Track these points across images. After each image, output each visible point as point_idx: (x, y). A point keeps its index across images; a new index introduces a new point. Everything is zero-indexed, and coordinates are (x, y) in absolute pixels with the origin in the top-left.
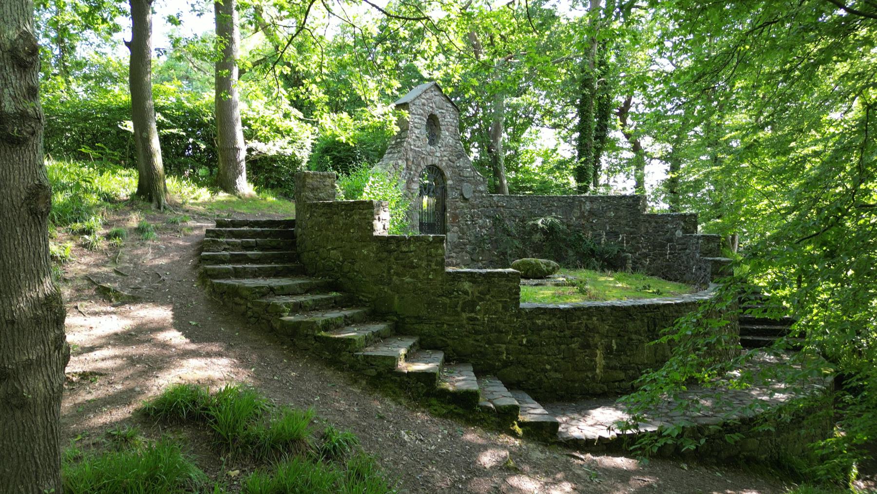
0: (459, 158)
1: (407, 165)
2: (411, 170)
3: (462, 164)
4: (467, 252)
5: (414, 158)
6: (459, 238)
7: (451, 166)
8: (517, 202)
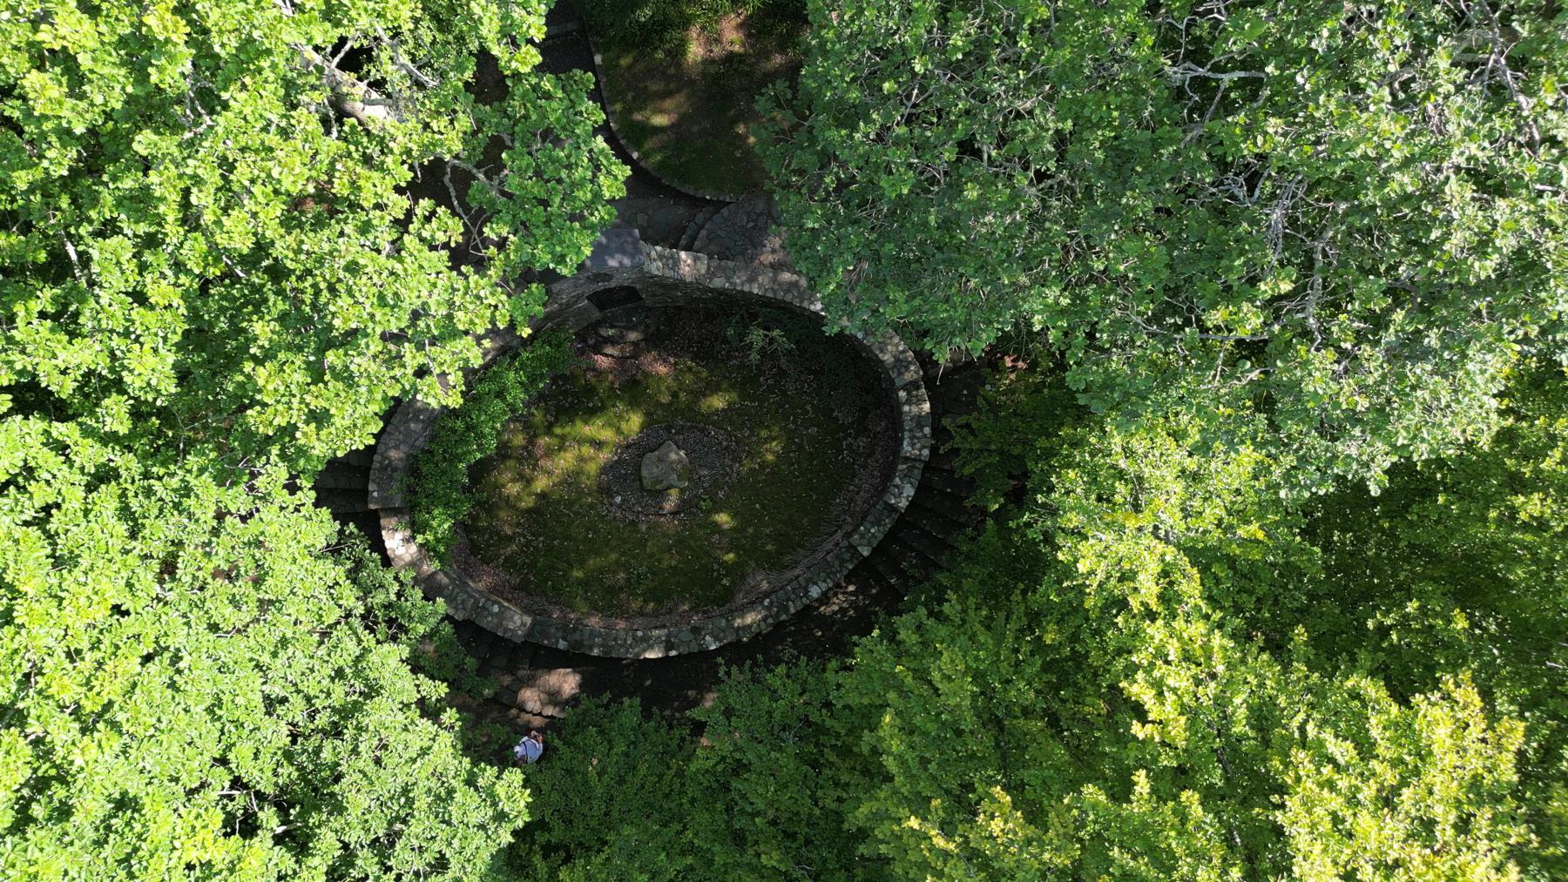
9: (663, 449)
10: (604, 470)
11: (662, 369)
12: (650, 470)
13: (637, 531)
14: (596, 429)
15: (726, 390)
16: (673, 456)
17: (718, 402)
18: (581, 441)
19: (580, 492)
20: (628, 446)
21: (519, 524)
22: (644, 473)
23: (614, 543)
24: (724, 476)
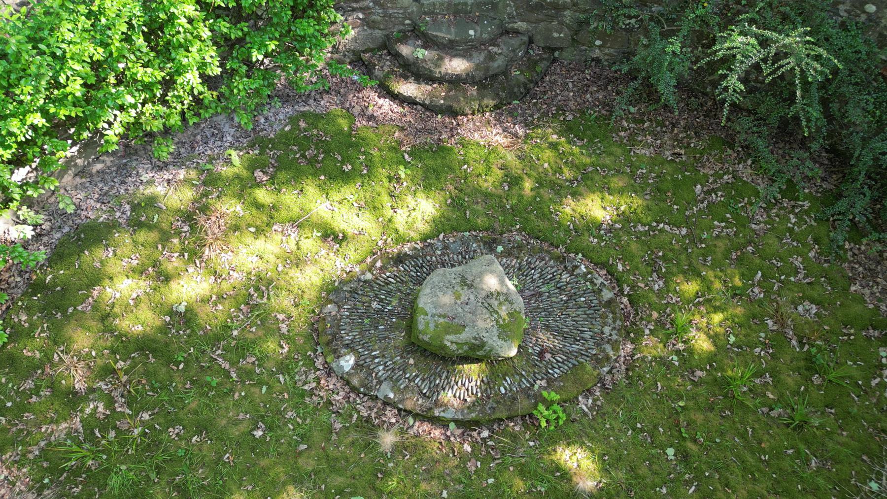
4: (561, 23)
9: (473, 268)
10: (333, 291)
11: (496, 137)
12: (436, 299)
13: (370, 446)
14: (336, 206)
15: (621, 192)
16: (491, 282)
17: (597, 208)
18: (299, 223)
19: (266, 321)
20: (400, 259)
21: (108, 372)
22: (425, 301)
23: (308, 464)
24: (598, 362)
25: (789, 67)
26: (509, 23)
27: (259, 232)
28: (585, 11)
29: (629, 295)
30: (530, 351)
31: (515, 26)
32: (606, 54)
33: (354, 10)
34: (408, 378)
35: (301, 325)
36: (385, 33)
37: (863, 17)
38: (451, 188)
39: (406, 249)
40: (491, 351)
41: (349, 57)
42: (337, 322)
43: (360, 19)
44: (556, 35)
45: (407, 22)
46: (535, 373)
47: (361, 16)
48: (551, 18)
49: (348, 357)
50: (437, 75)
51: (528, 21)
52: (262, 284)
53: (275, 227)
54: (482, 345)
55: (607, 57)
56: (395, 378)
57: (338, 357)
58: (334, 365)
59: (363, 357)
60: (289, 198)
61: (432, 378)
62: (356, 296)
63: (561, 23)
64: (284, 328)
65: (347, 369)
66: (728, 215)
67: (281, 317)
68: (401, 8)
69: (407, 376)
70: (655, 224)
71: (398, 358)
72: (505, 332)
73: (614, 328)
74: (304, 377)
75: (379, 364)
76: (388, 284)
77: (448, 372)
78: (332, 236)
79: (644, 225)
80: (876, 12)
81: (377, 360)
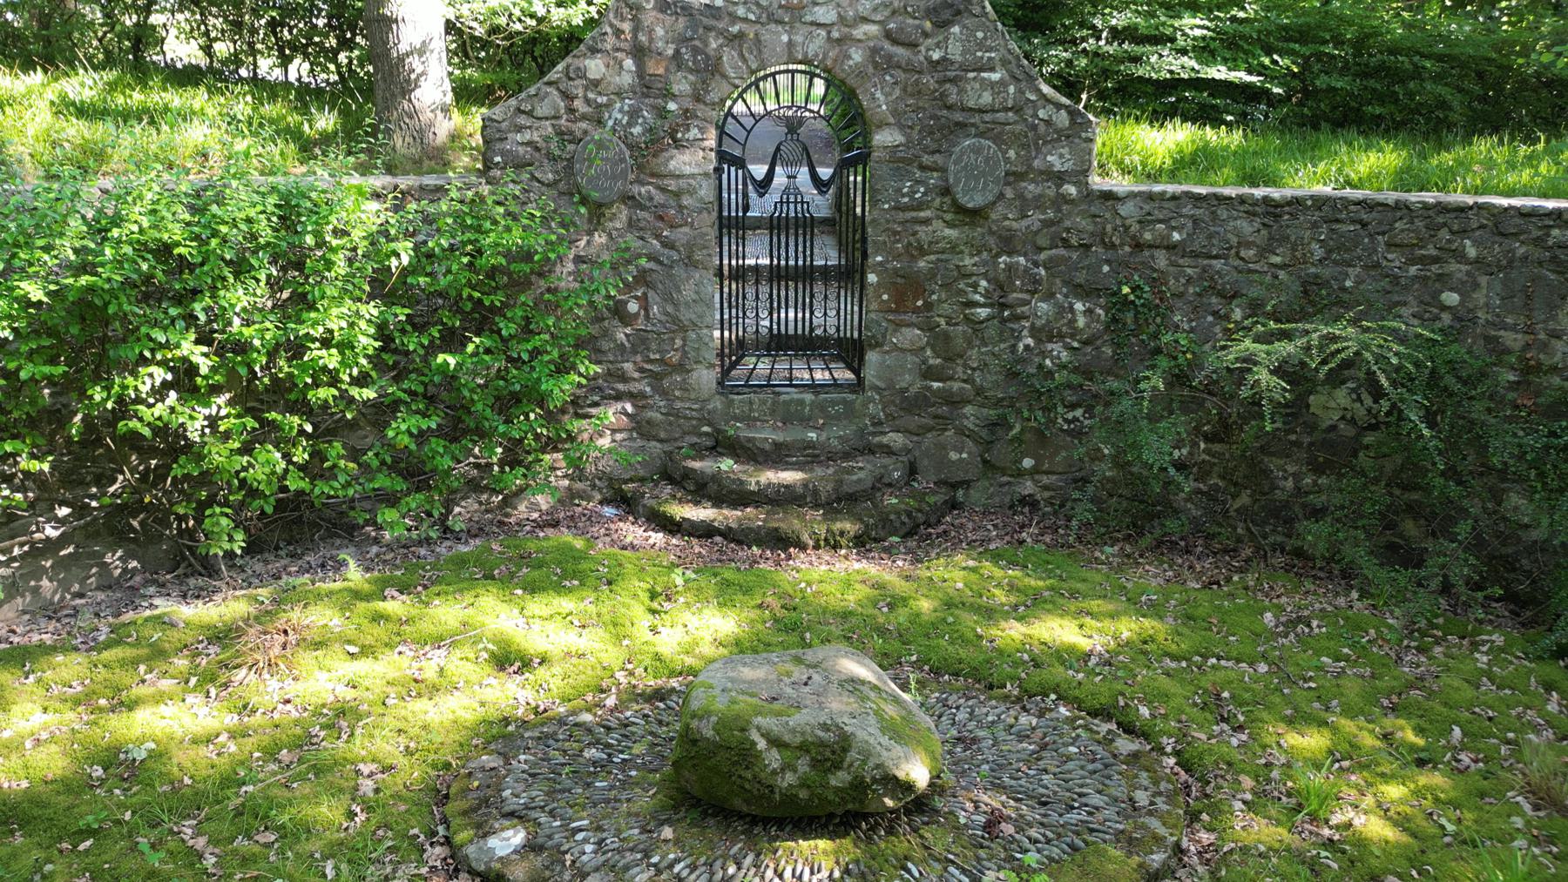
0: (942, 25)
1: (641, 72)
2: (669, 95)
3: (955, 51)
4: (961, 432)
5: (683, 40)
6: (929, 373)
7: (890, 64)
8: (1246, 227)
10: (503, 735)
25: (1350, 352)
26: (874, 434)
27: (366, 651)
28: (998, 403)
29: (1177, 753)
30: (963, 821)
31: (885, 440)
32: (1046, 488)
33: (618, 397)
34: (655, 865)
35: (412, 773)
36: (667, 447)
37: (1446, 318)
38: (775, 603)
39: (674, 683)
40: (864, 762)
41: (600, 490)
42: (494, 780)
43: (626, 414)
44: (954, 456)
45: (706, 429)
46: (979, 859)
47: (629, 408)
48: (942, 422)
49: (510, 833)
50: (753, 487)
51: (906, 431)
52: (342, 716)
53: (400, 648)
54: (844, 742)
55: (1047, 494)
56: (620, 864)
57: (485, 835)
58: (471, 850)
59: (548, 831)
60: (446, 612)
61: (718, 863)
62: (551, 742)
63: (961, 432)
64: (367, 786)
65: (500, 853)
66: (1346, 650)
67: (365, 769)
68: (696, 401)
69: (655, 860)
70: (1197, 658)
71: (636, 831)
72: (899, 732)
73: (1160, 794)
74: (389, 869)
75: (586, 841)
76: (626, 726)
77: (758, 855)
78: (518, 664)
79: (1174, 658)
80: (1462, 303)
81: (579, 837)
